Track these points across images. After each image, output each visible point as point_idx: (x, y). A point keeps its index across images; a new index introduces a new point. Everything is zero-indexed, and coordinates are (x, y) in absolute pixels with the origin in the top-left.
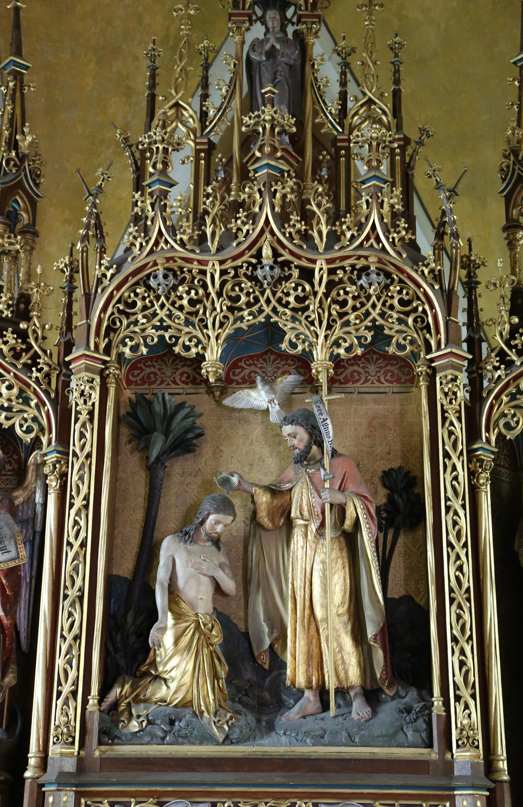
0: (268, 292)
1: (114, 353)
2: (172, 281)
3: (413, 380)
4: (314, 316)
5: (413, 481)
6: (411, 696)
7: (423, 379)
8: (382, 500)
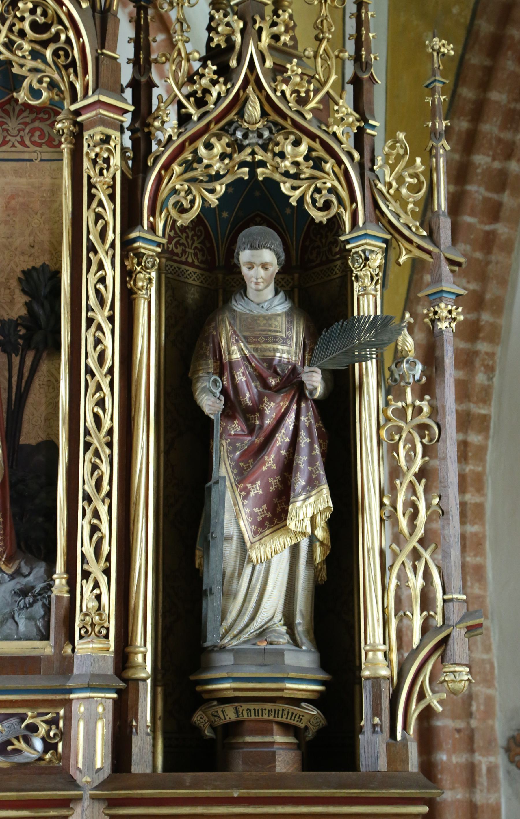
3: (53, 143)
7: (66, 140)
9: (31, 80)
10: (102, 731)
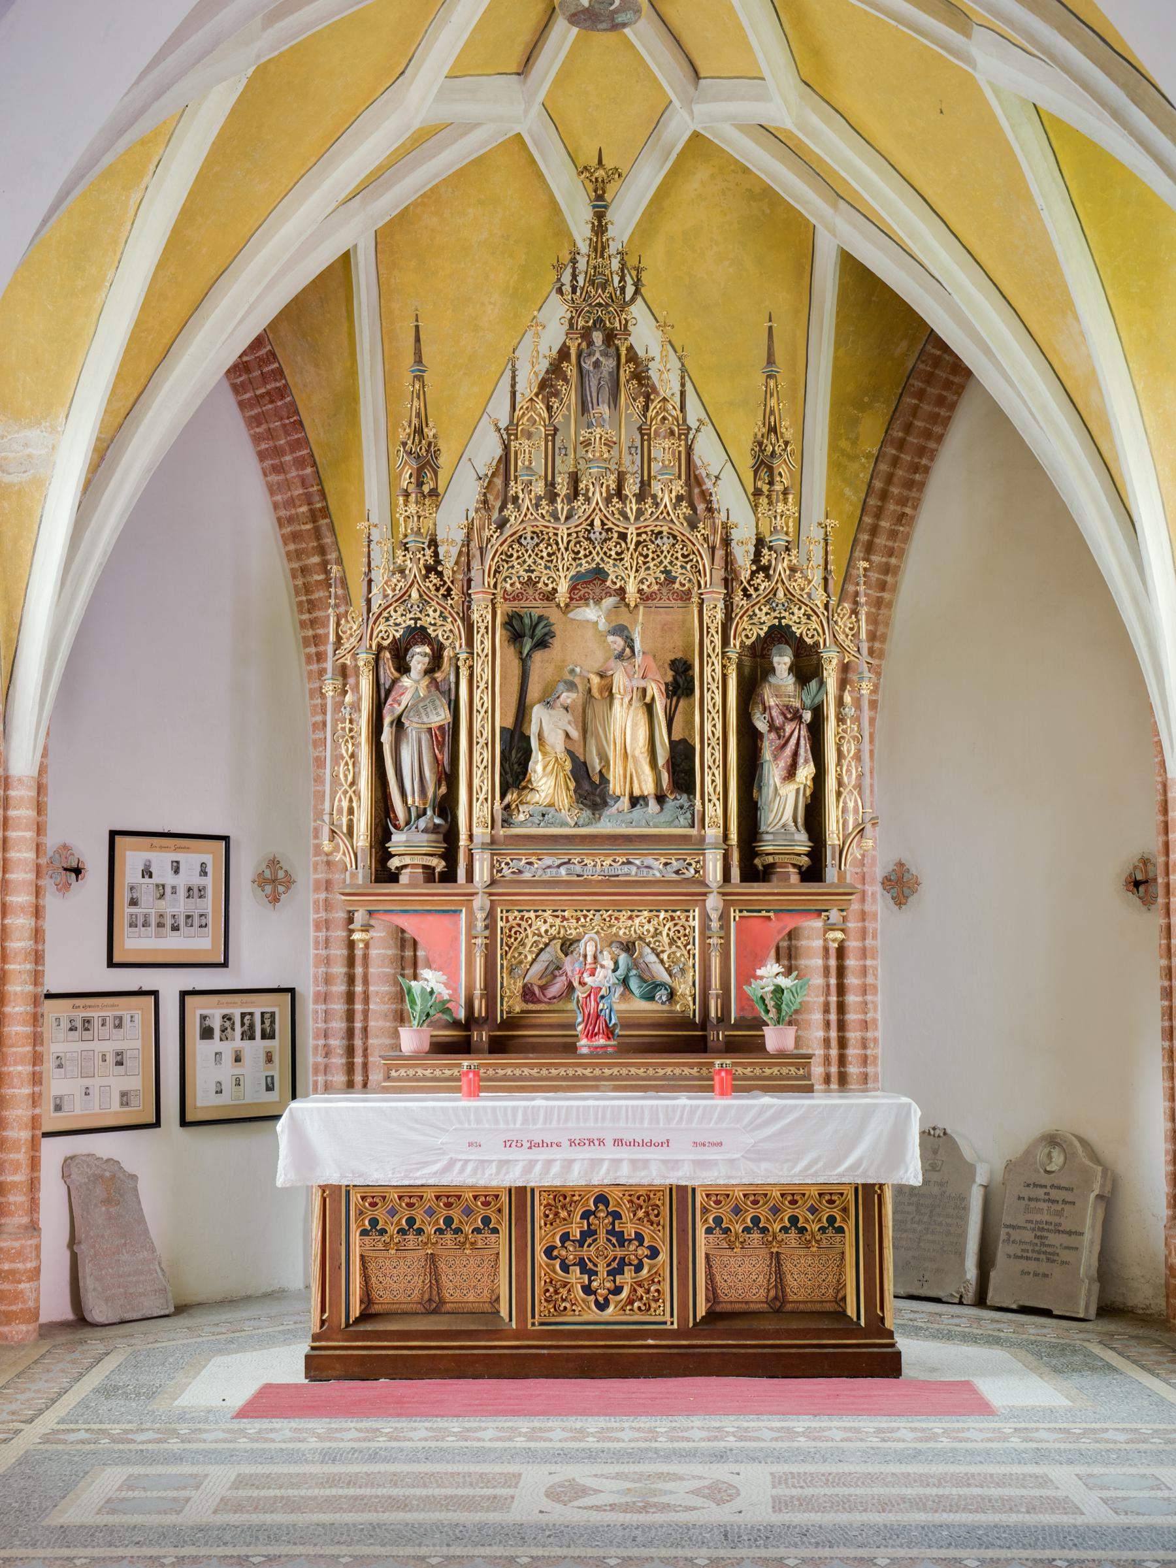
0: (598, 548)
1: (499, 587)
2: (536, 540)
4: (628, 565)
5: (688, 667)
6: (683, 799)
8: (669, 679)
9: (681, 579)
10: (719, 865)
